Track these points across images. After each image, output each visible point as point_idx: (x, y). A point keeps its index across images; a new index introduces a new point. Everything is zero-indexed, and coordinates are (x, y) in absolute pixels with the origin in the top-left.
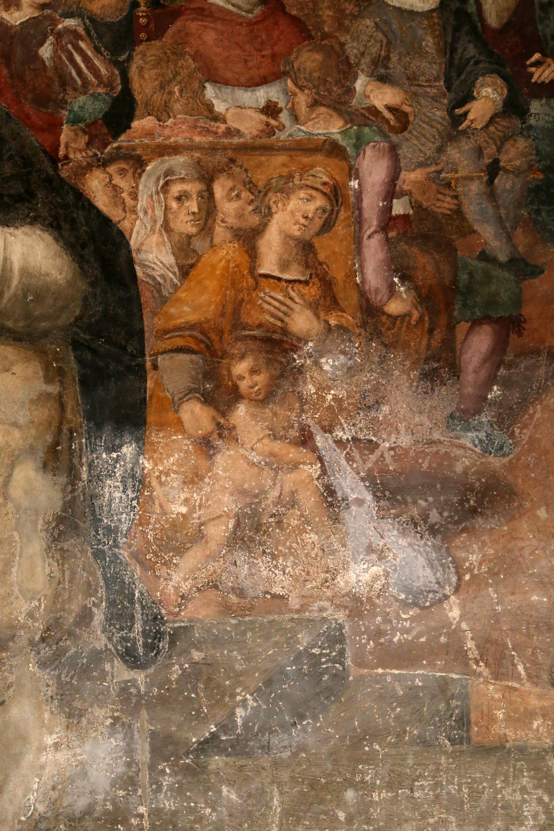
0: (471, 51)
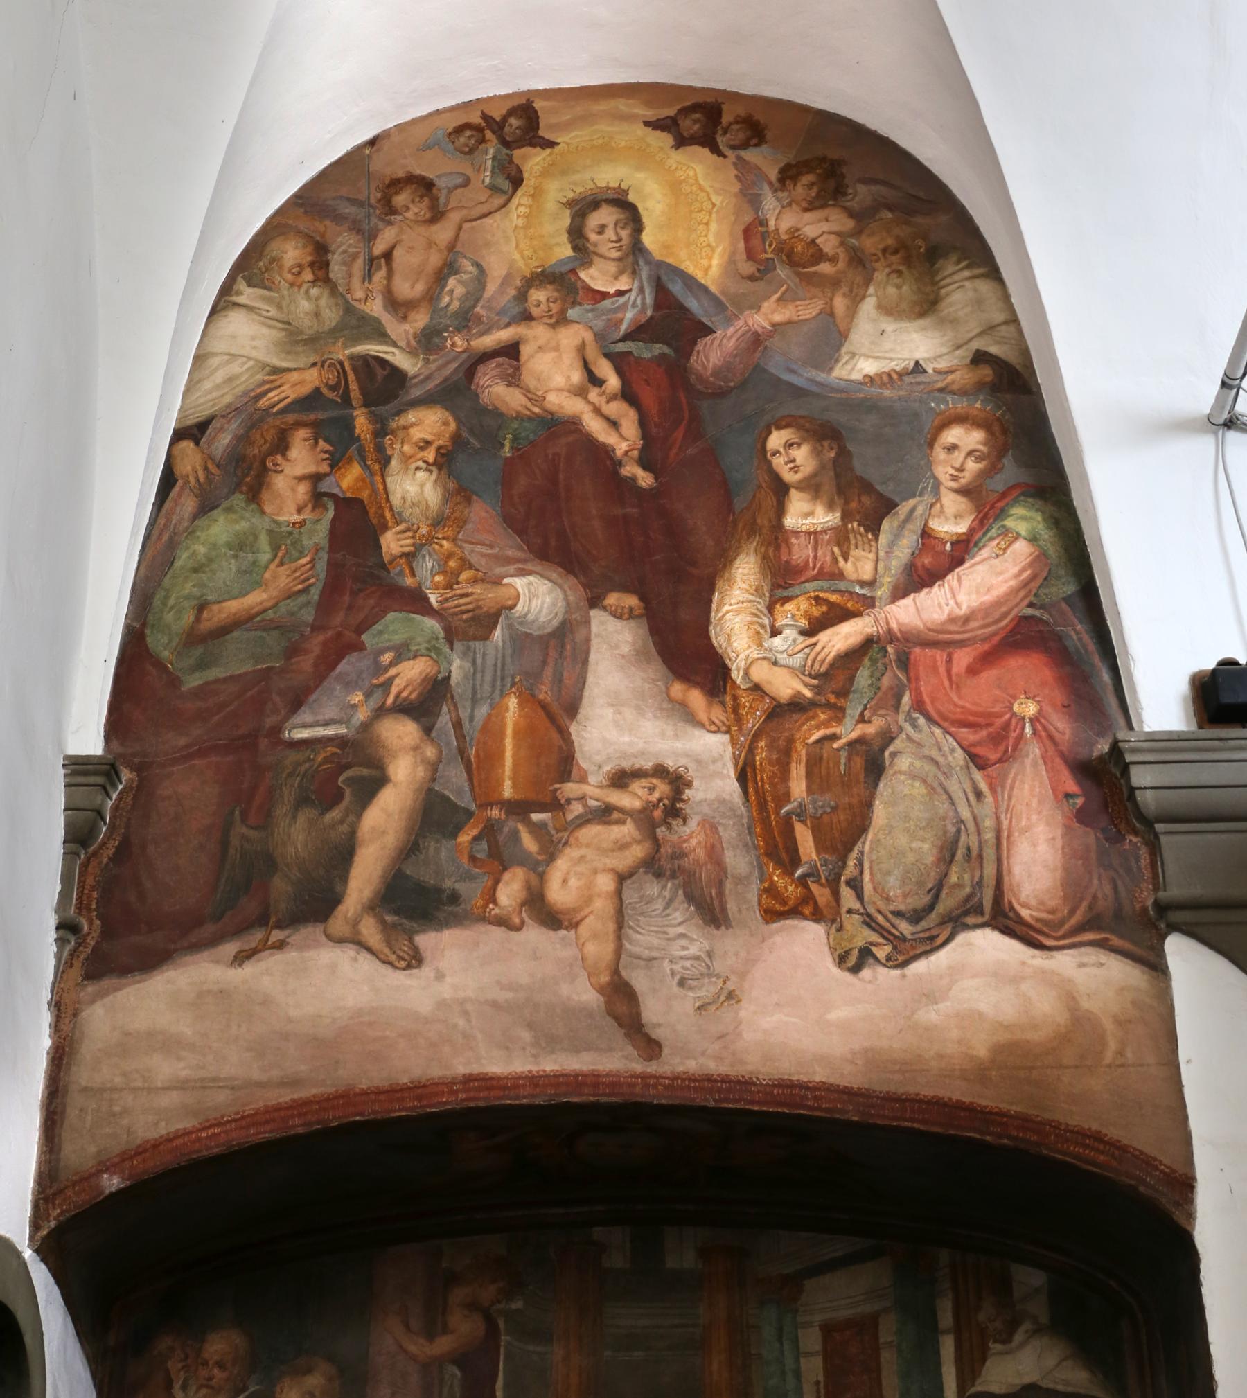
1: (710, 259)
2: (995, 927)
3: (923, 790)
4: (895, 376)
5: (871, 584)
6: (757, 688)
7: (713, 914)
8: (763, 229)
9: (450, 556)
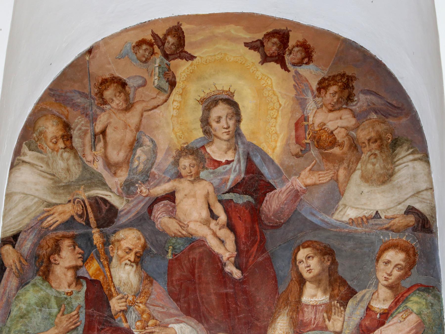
1: (276, 142)
4: (365, 220)
8: (306, 123)
9: (143, 312)
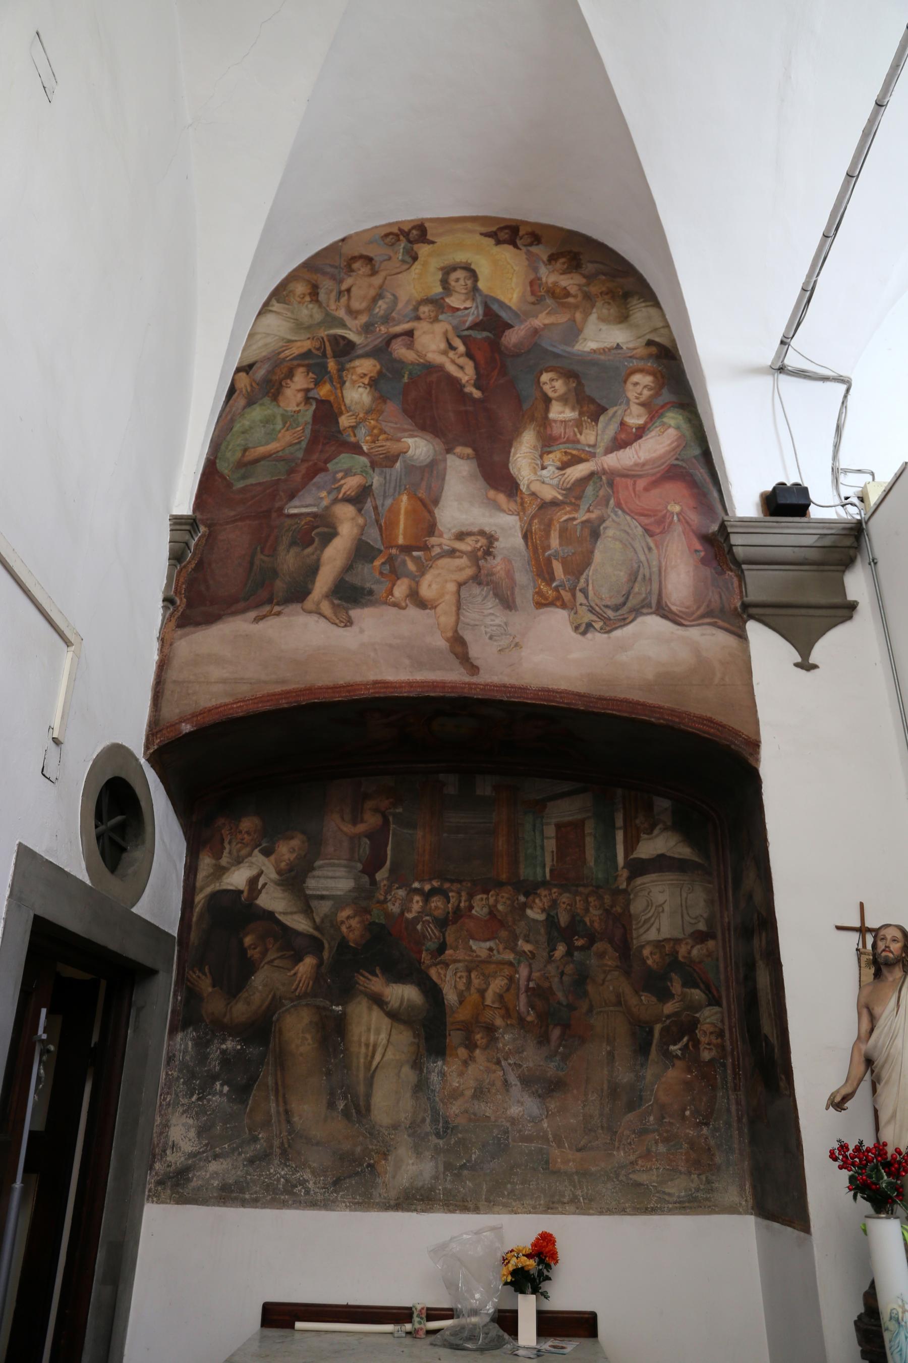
0: (556, 934)
2: (658, 615)
3: (621, 546)
5: (594, 446)
6: (533, 494)
7: (508, 604)
9: (374, 428)
